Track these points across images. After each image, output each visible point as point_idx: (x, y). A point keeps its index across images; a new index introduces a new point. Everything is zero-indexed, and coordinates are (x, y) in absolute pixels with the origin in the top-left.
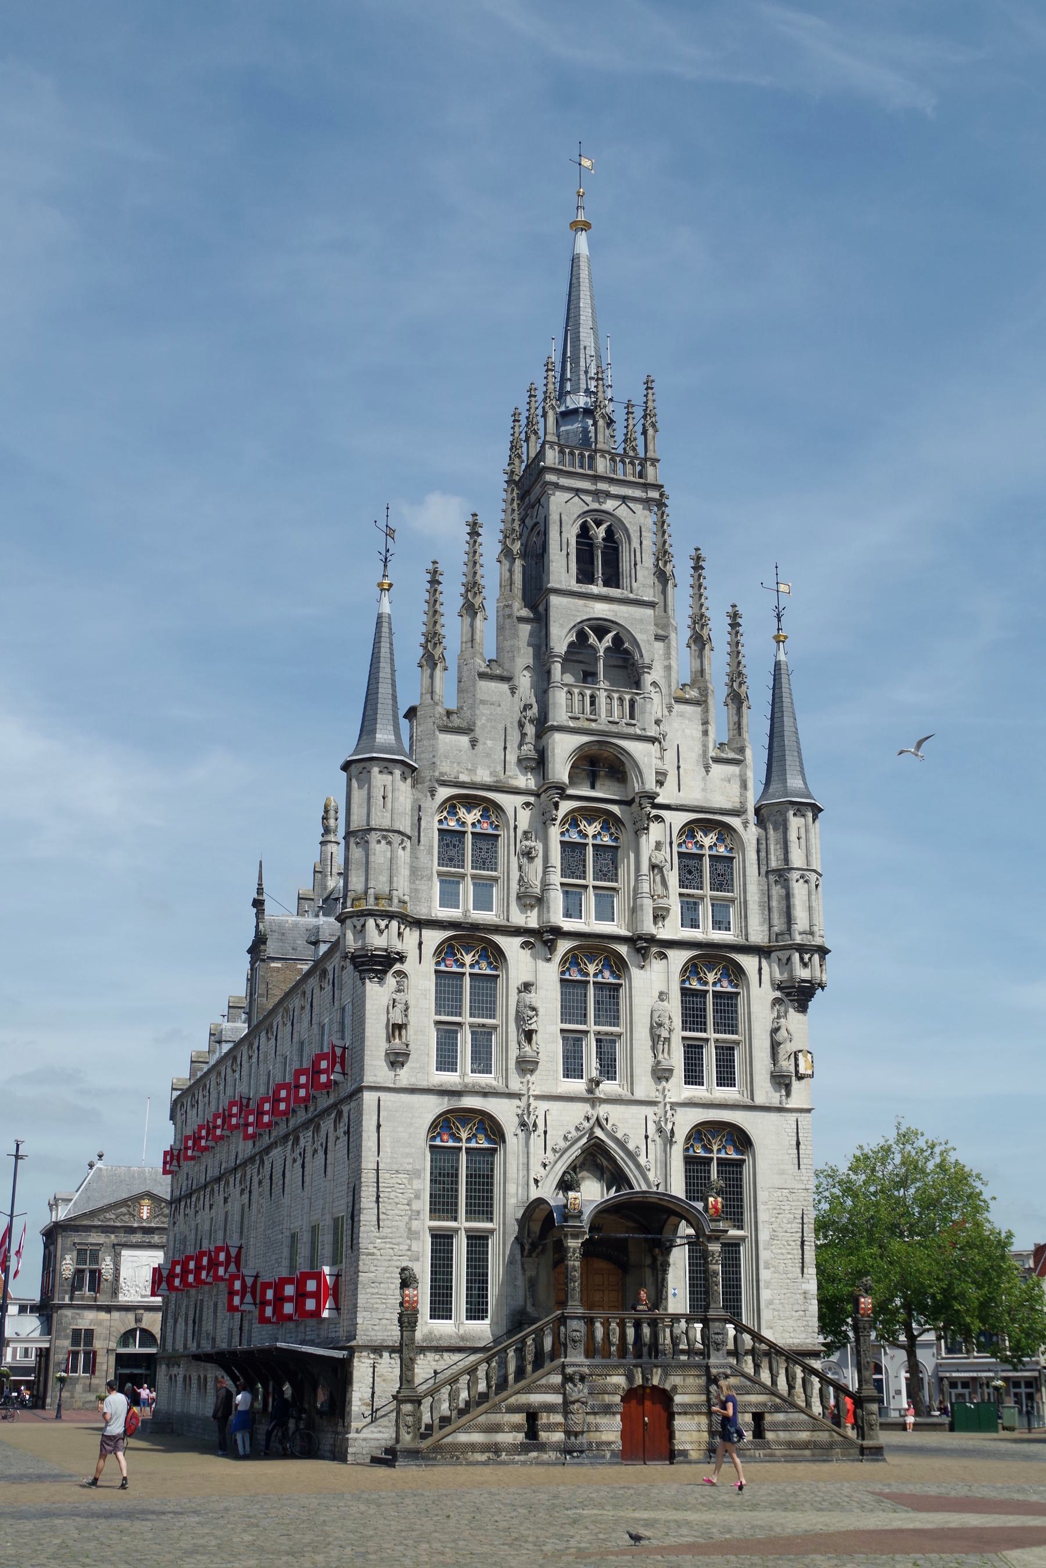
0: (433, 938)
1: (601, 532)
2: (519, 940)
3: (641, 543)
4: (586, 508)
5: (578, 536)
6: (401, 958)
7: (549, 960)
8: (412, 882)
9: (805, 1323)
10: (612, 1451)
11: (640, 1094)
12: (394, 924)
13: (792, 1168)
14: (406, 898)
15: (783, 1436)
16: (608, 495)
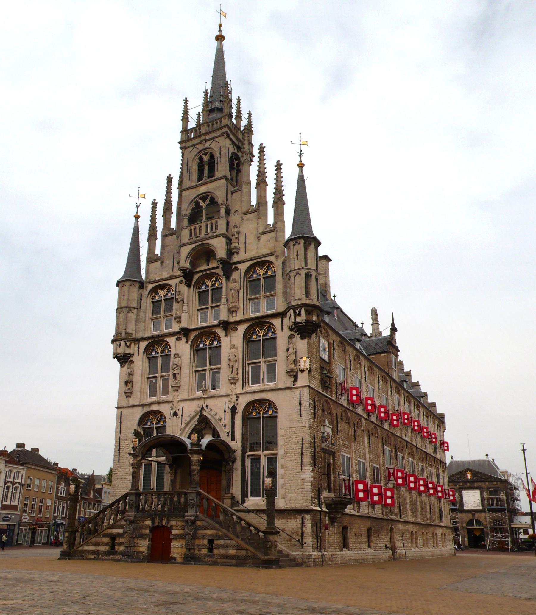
0: (143, 345)
1: (206, 158)
2: (174, 338)
3: (220, 154)
4: (198, 151)
5: (199, 164)
6: (131, 355)
7: (187, 342)
8: (136, 325)
9: (302, 495)
10: (144, 557)
11: (223, 393)
12: (123, 343)
13: (296, 416)
14: (133, 332)
15: (222, 551)
16: (206, 141)
